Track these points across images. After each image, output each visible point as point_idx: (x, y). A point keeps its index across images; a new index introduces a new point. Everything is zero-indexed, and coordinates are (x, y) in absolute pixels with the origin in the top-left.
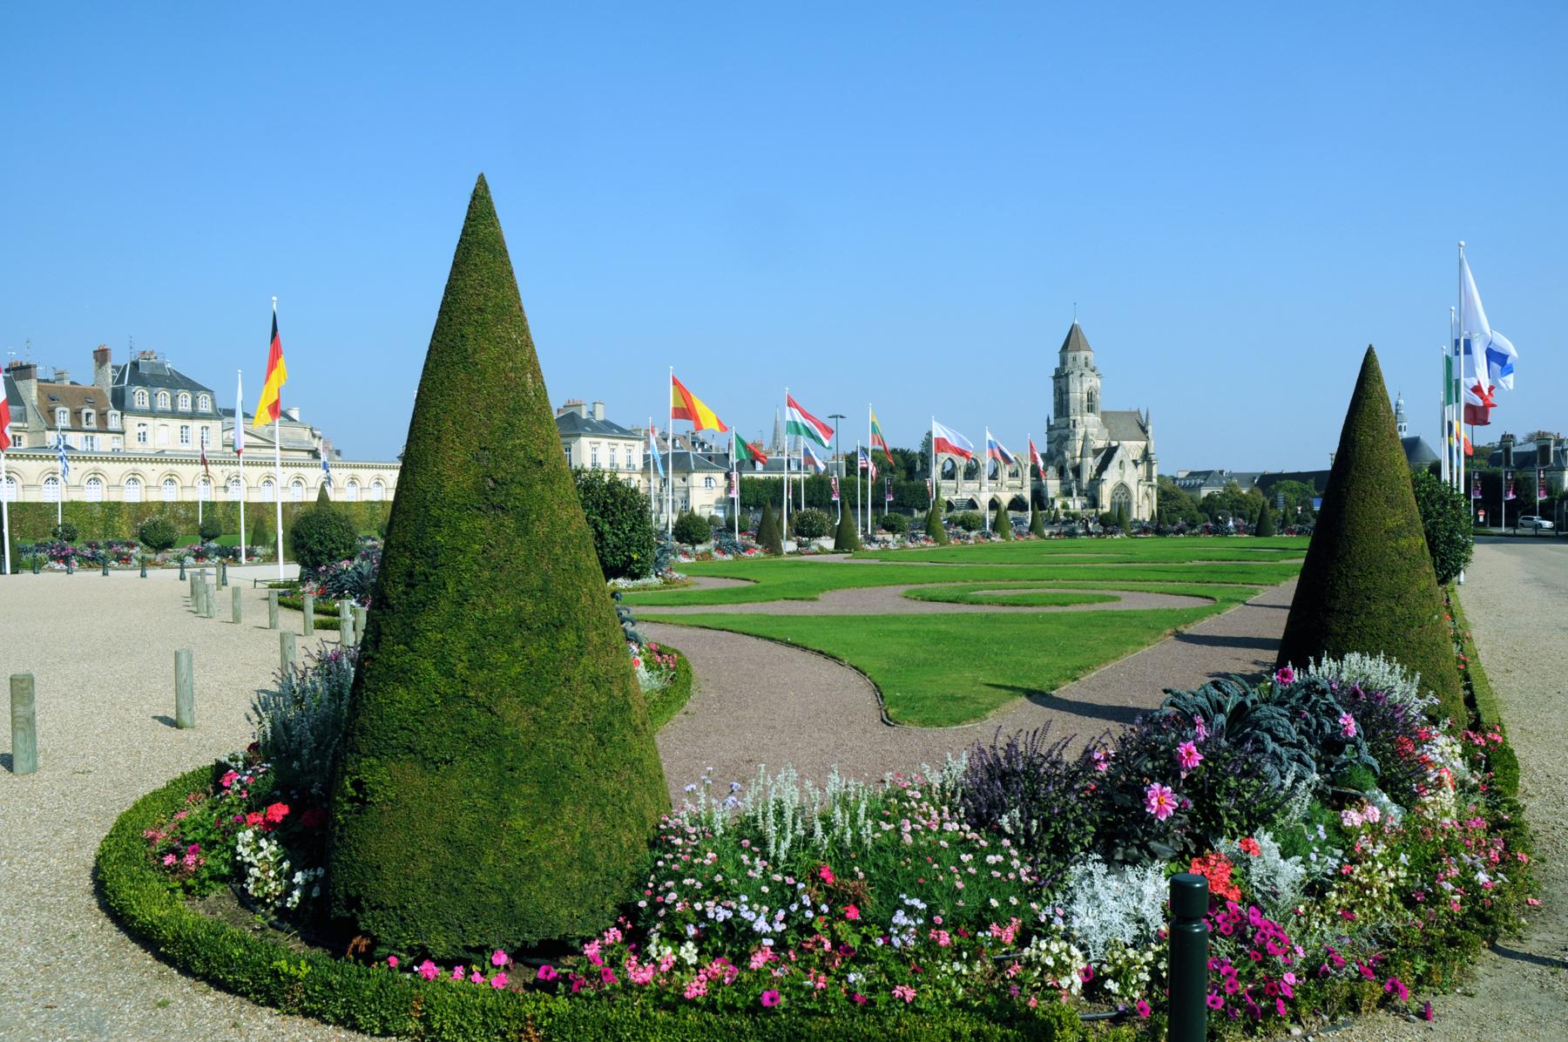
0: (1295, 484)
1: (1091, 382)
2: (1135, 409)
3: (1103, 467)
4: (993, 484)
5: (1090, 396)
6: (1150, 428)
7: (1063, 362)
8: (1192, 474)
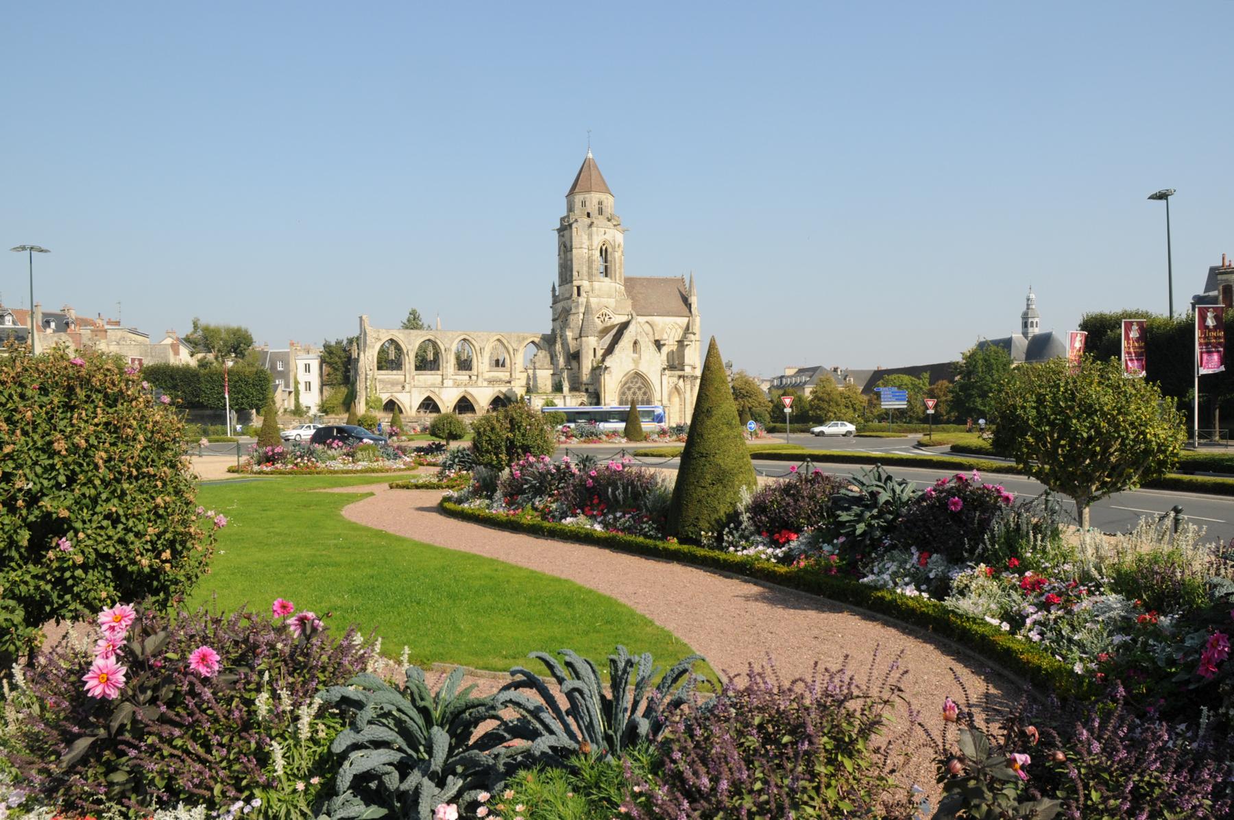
0: (906, 379)
1: (605, 234)
2: (679, 276)
3: (610, 350)
4: (463, 376)
5: (604, 253)
6: (694, 300)
7: (571, 209)
8: (801, 371)
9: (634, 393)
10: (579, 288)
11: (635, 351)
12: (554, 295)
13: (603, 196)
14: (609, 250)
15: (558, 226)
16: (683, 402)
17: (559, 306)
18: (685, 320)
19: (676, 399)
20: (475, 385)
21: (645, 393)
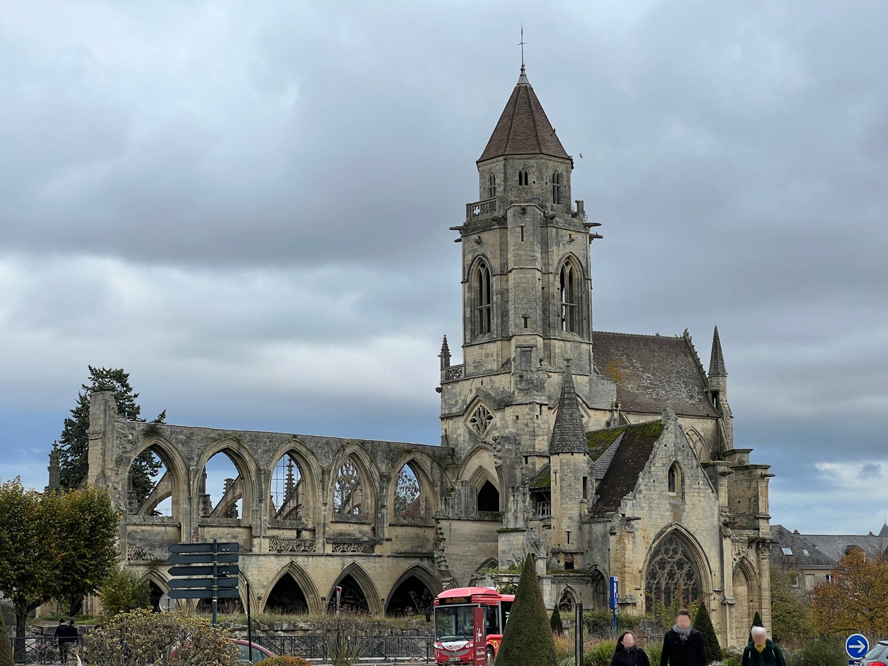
2: (673, 332)
9: (671, 575)
11: (671, 487)
13: (561, 168)
14: (577, 275)
15: (462, 220)
16: (754, 590)
17: (465, 390)
18: (710, 424)
19: (743, 589)
20: (309, 550)
21: (689, 575)
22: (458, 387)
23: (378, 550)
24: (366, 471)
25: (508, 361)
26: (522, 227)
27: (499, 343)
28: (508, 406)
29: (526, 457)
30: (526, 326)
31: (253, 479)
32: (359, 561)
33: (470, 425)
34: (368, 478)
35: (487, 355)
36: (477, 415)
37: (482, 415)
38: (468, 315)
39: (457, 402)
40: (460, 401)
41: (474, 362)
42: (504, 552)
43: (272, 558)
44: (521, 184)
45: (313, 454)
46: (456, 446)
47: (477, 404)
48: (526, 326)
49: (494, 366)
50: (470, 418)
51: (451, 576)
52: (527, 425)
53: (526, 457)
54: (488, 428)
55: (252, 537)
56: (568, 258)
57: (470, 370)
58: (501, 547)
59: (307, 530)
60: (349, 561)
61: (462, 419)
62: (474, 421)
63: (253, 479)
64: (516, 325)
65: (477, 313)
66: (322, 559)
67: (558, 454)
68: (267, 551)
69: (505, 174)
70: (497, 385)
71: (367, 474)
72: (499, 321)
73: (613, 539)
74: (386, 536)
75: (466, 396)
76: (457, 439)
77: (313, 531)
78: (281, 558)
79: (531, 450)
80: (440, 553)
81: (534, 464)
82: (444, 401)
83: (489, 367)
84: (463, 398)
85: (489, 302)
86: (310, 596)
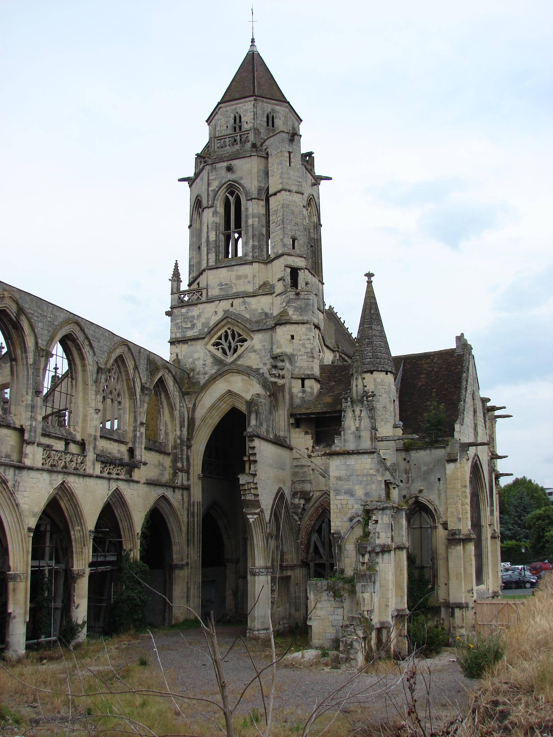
10: (294, 272)
12: (176, 291)
22: (195, 311)
23: (137, 474)
24: (128, 379)
25: (265, 284)
26: (290, 153)
27: (256, 265)
28: (281, 324)
29: (303, 380)
30: (294, 248)
31: (31, 361)
32: (123, 487)
33: (213, 349)
34: (129, 389)
35: (239, 278)
36: (223, 338)
37: (230, 338)
38: (212, 237)
39: (193, 326)
40: (199, 326)
41: (221, 284)
42: (339, 479)
43: (45, 475)
44: (268, 125)
45: (91, 345)
46: (193, 370)
47: (223, 326)
48: (294, 248)
49: (250, 289)
50: (213, 341)
51: (259, 506)
52: (304, 345)
53: (303, 380)
54: (240, 351)
55: (23, 442)
56: (310, 201)
57: (214, 292)
58: (333, 473)
59: (75, 442)
60: (114, 485)
61: (200, 343)
62: (217, 344)
63: (31, 361)
64: (284, 245)
65: (222, 237)
66: (91, 482)
67: (372, 372)
68: (40, 465)
69: (255, 114)
70: (253, 307)
71: (128, 384)
72: (256, 243)
73: (450, 467)
74: (143, 460)
75: (210, 319)
76: (193, 363)
77: (82, 445)
78: (54, 476)
79: (309, 373)
80: (250, 479)
81: (311, 387)
82: (175, 325)
83: (241, 289)
84: (203, 320)
85: (238, 225)
86: (78, 528)
